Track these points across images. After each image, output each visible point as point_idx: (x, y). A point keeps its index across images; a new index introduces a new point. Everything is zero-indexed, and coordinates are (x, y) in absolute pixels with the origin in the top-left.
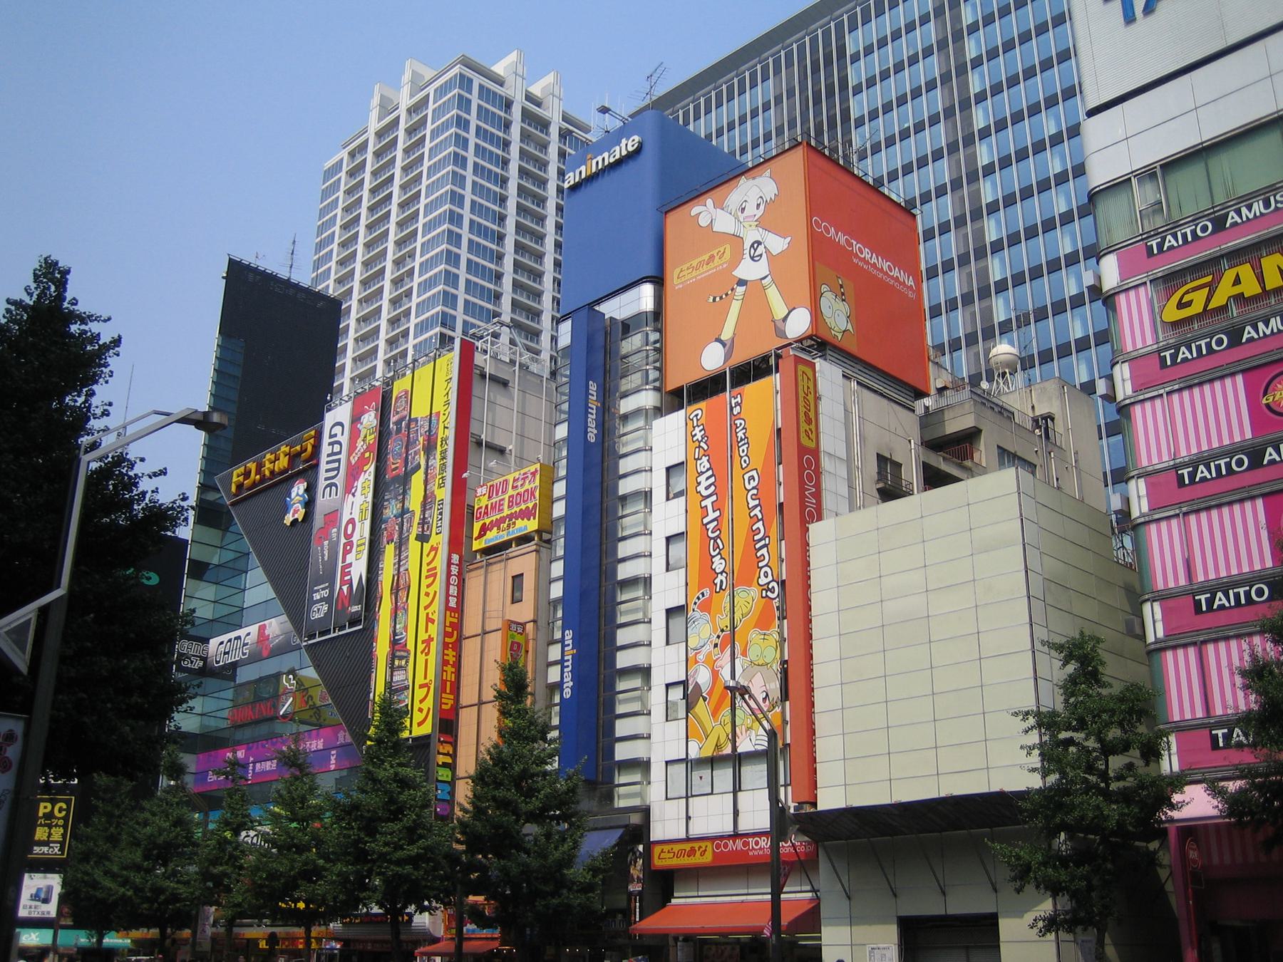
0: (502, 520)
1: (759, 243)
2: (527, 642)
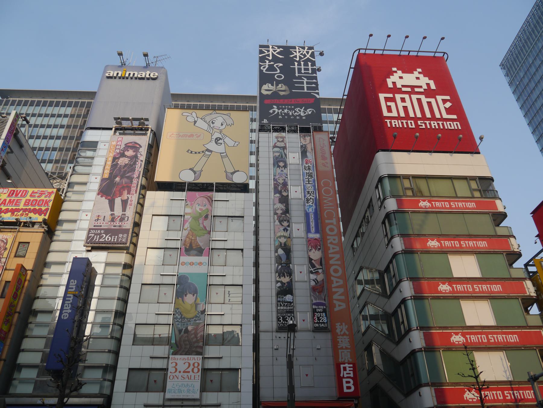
0: (18, 210)
1: (220, 139)
2: (25, 280)
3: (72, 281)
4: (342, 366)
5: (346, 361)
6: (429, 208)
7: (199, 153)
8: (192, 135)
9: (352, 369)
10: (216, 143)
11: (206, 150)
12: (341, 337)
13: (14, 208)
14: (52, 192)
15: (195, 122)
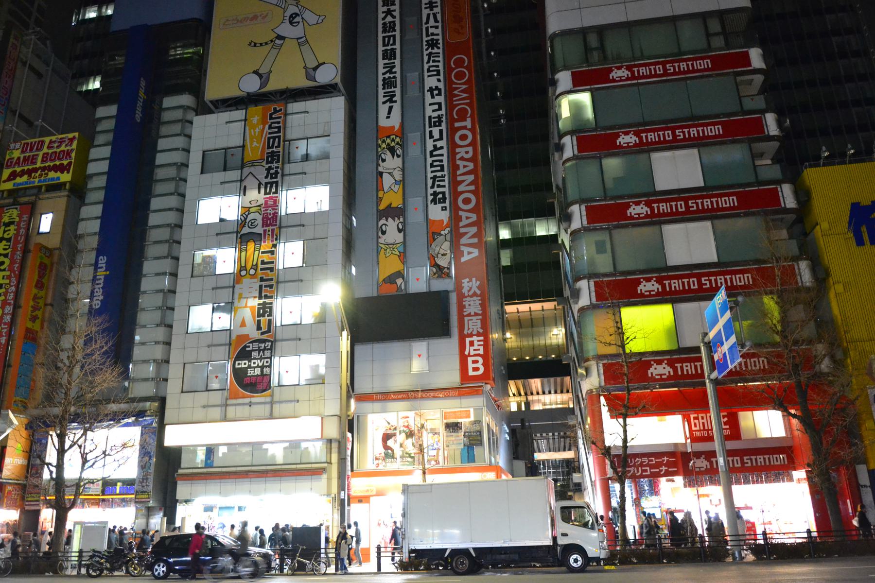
0: (35, 170)
1: (297, 15)
2: (52, 264)
3: (101, 257)
4: (468, 340)
5: (475, 332)
6: (628, 79)
7: (266, 44)
8: (255, 18)
9: (482, 343)
10: (291, 23)
11: (276, 38)
12: (468, 299)
13: (30, 167)
14: (74, 138)
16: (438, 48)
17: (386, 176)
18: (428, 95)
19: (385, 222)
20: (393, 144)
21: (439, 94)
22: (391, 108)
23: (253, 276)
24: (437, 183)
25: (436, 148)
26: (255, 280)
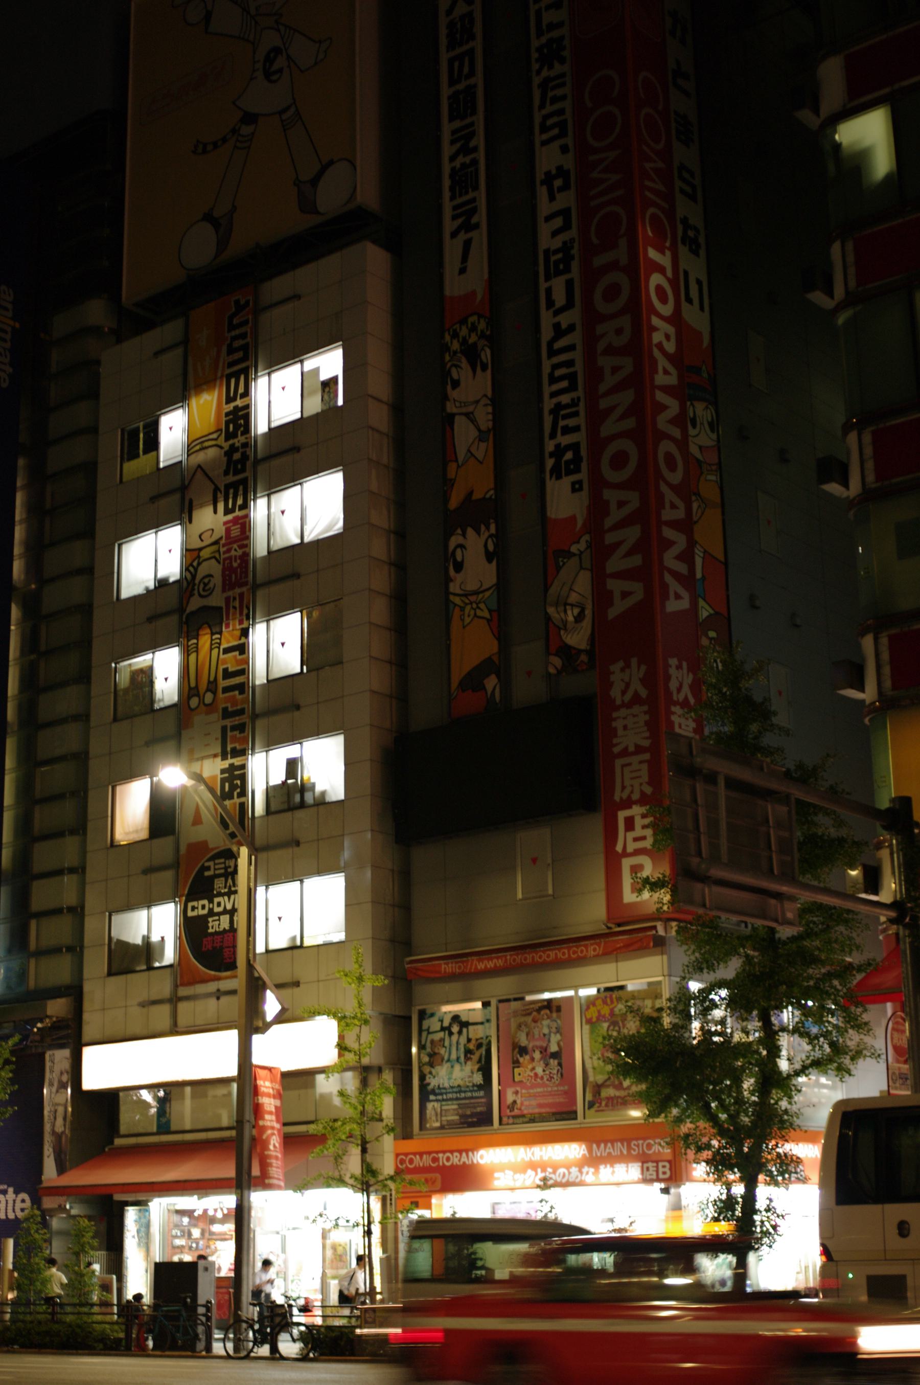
4: (622, 815)
5: (636, 796)
7: (224, 140)
10: (268, 75)
12: (623, 712)
15: (208, 16)
16: (562, 61)
17: (461, 424)
18: (542, 192)
19: (460, 540)
20: (473, 339)
21: (565, 187)
22: (467, 244)
23: (210, 708)
24: (562, 423)
25: (559, 332)
26: (215, 717)
